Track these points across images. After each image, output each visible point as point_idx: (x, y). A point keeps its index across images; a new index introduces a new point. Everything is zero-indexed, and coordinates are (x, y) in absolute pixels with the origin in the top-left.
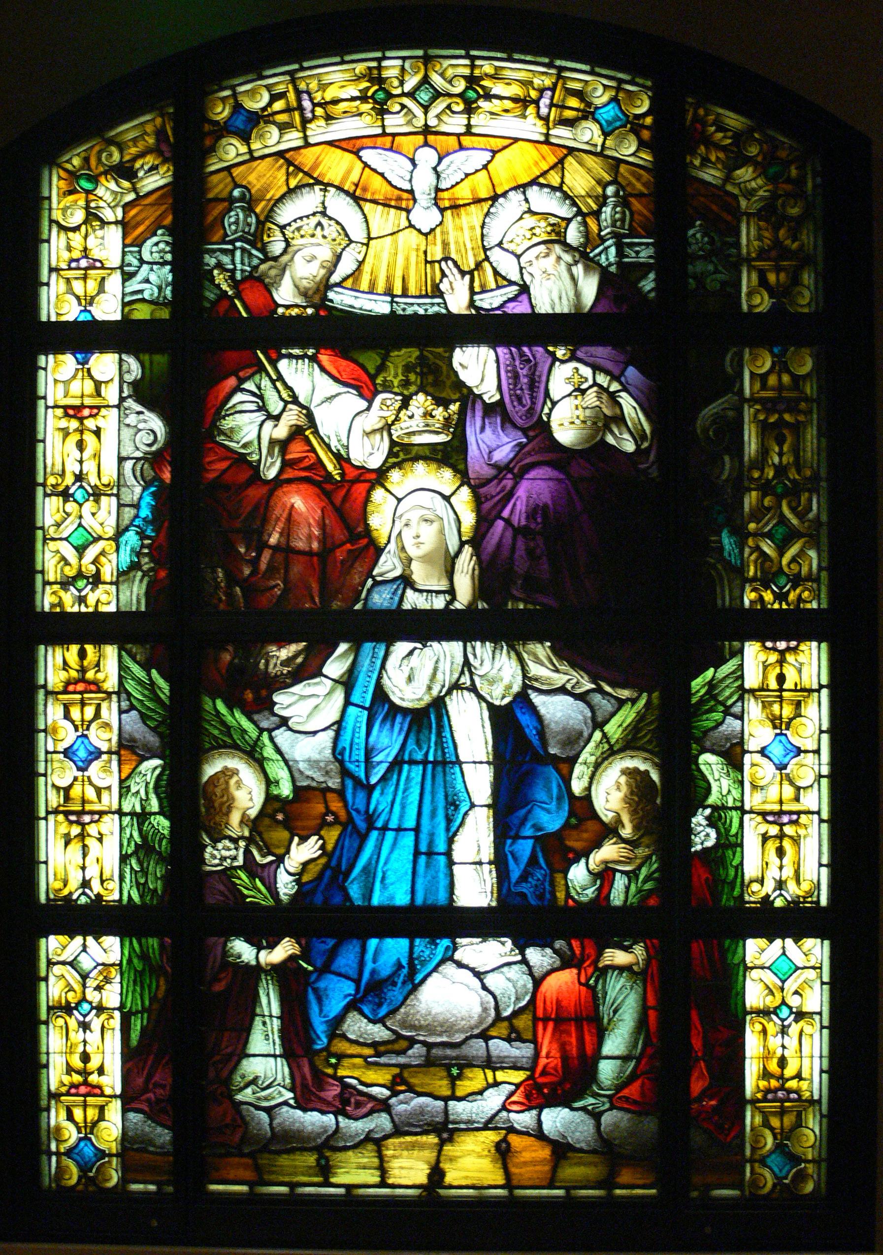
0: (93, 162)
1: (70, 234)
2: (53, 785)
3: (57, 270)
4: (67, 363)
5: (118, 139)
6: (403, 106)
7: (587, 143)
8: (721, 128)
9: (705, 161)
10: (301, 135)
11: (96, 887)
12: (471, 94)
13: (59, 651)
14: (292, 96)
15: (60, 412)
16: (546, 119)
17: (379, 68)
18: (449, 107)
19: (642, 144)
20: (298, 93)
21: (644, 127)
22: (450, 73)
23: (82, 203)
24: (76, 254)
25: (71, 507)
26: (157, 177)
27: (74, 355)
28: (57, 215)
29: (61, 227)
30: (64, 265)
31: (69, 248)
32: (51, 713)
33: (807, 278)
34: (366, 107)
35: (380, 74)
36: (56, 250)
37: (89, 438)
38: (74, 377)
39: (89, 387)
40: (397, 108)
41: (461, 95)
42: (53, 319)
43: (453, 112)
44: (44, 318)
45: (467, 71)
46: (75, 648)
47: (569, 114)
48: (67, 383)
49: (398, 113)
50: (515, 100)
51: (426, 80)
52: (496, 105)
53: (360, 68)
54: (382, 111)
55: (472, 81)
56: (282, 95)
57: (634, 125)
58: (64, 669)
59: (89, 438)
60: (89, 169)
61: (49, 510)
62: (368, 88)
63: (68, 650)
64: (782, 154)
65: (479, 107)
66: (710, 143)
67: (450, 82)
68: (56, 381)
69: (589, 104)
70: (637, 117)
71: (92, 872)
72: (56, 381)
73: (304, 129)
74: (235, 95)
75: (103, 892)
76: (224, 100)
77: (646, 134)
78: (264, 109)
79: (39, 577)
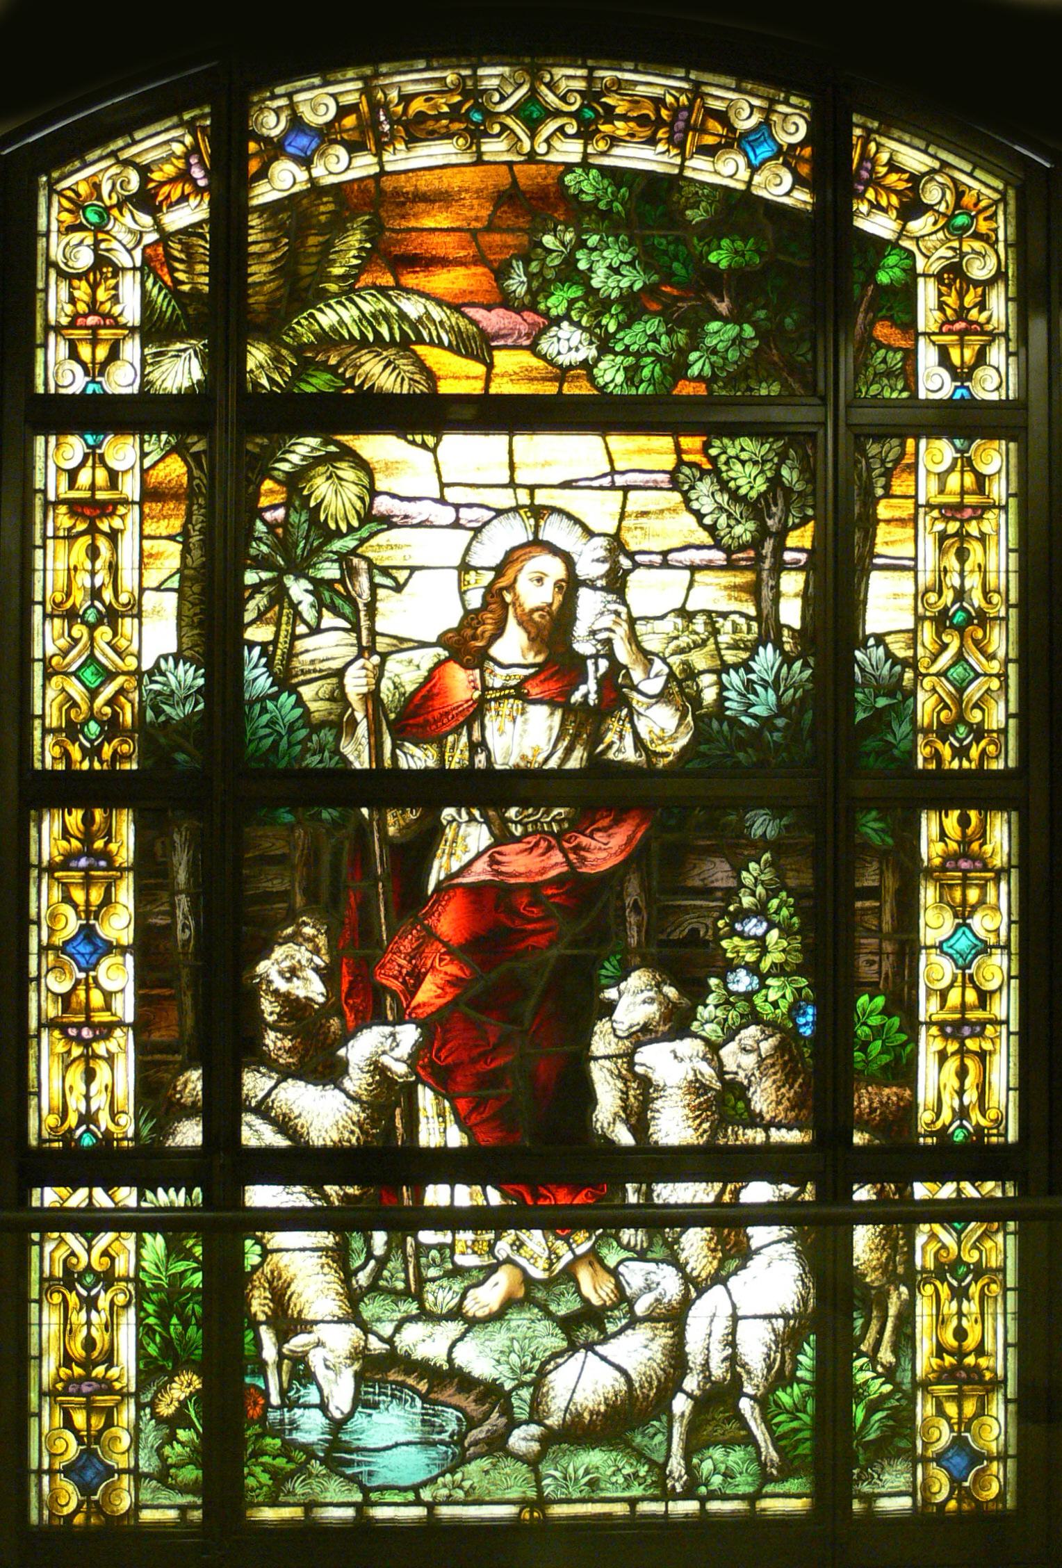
0: (106, 188)
1: (76, 283)
2: (48, 990)
3: (58, 329)
4: (73, 448)
5: (138, 160)
6: (504, 127)
7: (731, 177)
8: (893, 167)
9: (876, 206)
10: (375, 160)
11: (104, 1120)
12: (589, 114)
13: (57, 814)
14: (364, 107)
15: (63, 509)
16: (681, 146)
17: (476, 78)
18: (561, 129)
19: (798, 181)
20: (374, 106)
21: (800, 158)
22: (563, 86)
23: (90, 240)
24: (82, 307)
25: (79, 630)
26: (188, 210)
27: (82, 437)
28: (56, 253)
29: (62, 274)
30: (64, 321)
31: (73, 300)
32: (44, 897)
33: (997, 354)
34: (456, 126)
35: (475, 85)
36: (57, 302)
37: (103, 543)
38: (82, 465)
39: (102, 476)
40: (497, 129)
41: (575, 115)
42: (52, 391)
43: (567, 136)
44: (40, 390)
45: (581, 85)
46: (78, 814)
47: (709, 140)
48: (73, 475)
49: (498, 135)
50: (642, 120)
51: (533, 94)
52: (621, 128)
53: (451, 77)
54: (476, 135)
55: (591, 96)
56: (352, 109)
57: (786, 155)
58: (64, 838)
59: (103, 543)
60: (100, 198)
61: (48, 637)
62: (460, 104)
63: (70, 813)
64: (968, 200)
65: (599, 131)
66: (876, 183)
67: (563, 99)
68: (59, 468)
69: (732, 129)
70: (792, 147)
71: (100, 1101)
72: (59, 468)
73: (378, 154)
74: (292, 106)
75: (112, 1127)
76: (277, 111)
77: (805, 170)
78: (329, 125)
79: (37, 723)
